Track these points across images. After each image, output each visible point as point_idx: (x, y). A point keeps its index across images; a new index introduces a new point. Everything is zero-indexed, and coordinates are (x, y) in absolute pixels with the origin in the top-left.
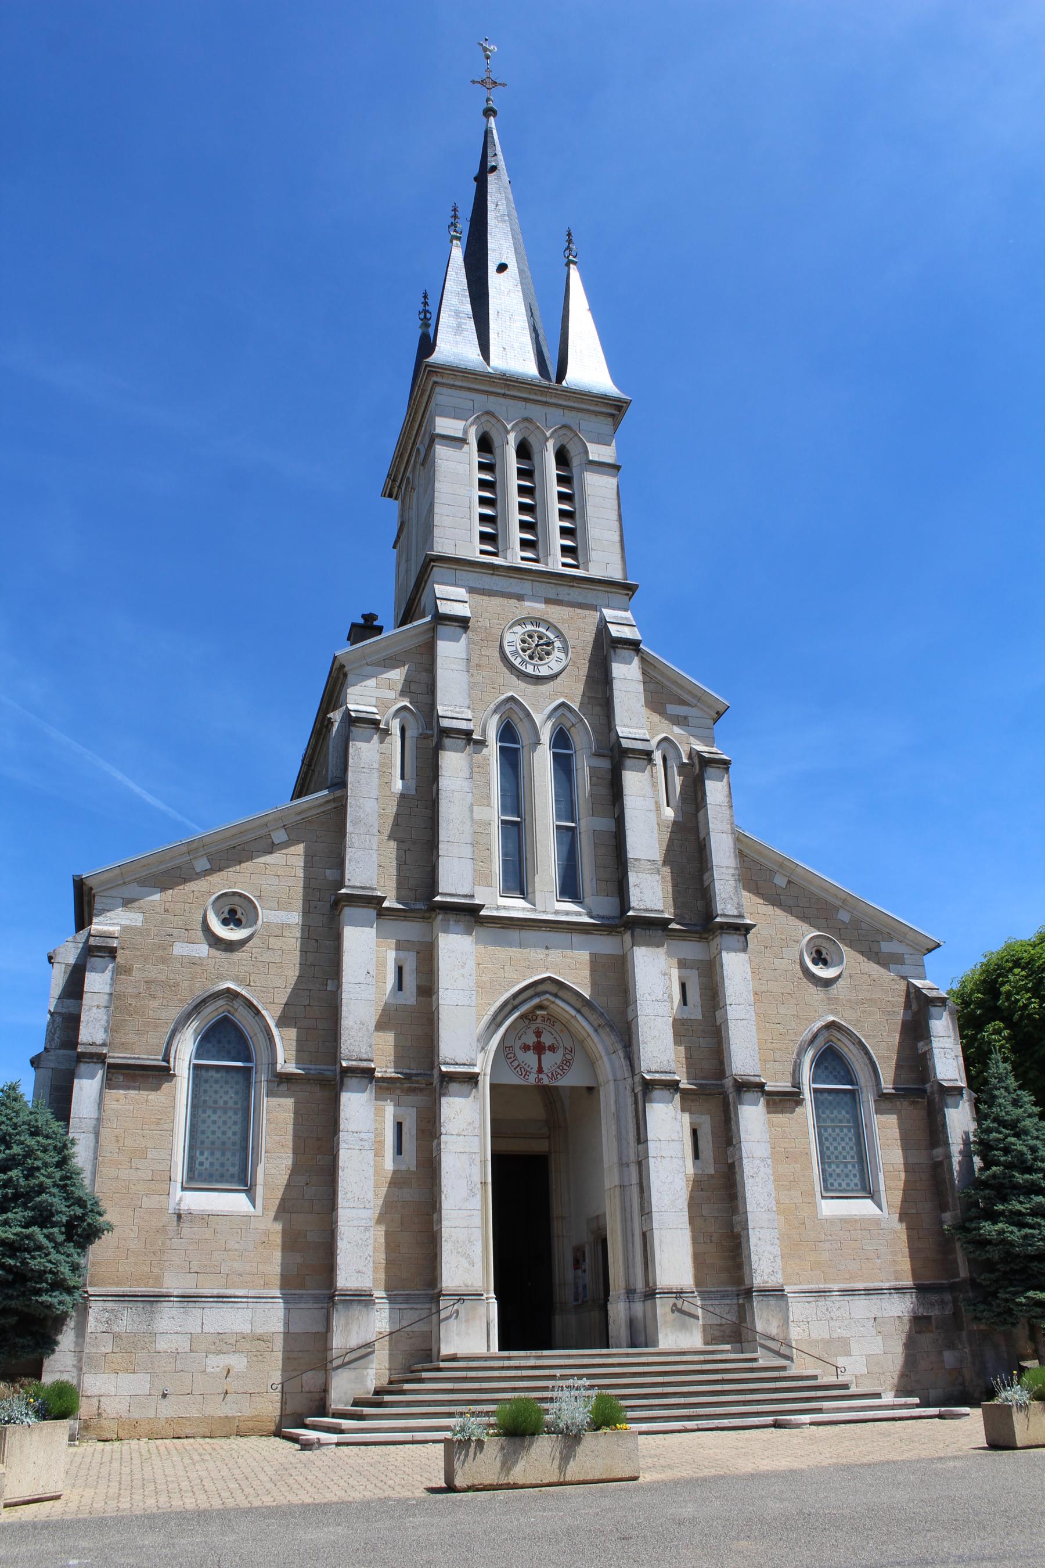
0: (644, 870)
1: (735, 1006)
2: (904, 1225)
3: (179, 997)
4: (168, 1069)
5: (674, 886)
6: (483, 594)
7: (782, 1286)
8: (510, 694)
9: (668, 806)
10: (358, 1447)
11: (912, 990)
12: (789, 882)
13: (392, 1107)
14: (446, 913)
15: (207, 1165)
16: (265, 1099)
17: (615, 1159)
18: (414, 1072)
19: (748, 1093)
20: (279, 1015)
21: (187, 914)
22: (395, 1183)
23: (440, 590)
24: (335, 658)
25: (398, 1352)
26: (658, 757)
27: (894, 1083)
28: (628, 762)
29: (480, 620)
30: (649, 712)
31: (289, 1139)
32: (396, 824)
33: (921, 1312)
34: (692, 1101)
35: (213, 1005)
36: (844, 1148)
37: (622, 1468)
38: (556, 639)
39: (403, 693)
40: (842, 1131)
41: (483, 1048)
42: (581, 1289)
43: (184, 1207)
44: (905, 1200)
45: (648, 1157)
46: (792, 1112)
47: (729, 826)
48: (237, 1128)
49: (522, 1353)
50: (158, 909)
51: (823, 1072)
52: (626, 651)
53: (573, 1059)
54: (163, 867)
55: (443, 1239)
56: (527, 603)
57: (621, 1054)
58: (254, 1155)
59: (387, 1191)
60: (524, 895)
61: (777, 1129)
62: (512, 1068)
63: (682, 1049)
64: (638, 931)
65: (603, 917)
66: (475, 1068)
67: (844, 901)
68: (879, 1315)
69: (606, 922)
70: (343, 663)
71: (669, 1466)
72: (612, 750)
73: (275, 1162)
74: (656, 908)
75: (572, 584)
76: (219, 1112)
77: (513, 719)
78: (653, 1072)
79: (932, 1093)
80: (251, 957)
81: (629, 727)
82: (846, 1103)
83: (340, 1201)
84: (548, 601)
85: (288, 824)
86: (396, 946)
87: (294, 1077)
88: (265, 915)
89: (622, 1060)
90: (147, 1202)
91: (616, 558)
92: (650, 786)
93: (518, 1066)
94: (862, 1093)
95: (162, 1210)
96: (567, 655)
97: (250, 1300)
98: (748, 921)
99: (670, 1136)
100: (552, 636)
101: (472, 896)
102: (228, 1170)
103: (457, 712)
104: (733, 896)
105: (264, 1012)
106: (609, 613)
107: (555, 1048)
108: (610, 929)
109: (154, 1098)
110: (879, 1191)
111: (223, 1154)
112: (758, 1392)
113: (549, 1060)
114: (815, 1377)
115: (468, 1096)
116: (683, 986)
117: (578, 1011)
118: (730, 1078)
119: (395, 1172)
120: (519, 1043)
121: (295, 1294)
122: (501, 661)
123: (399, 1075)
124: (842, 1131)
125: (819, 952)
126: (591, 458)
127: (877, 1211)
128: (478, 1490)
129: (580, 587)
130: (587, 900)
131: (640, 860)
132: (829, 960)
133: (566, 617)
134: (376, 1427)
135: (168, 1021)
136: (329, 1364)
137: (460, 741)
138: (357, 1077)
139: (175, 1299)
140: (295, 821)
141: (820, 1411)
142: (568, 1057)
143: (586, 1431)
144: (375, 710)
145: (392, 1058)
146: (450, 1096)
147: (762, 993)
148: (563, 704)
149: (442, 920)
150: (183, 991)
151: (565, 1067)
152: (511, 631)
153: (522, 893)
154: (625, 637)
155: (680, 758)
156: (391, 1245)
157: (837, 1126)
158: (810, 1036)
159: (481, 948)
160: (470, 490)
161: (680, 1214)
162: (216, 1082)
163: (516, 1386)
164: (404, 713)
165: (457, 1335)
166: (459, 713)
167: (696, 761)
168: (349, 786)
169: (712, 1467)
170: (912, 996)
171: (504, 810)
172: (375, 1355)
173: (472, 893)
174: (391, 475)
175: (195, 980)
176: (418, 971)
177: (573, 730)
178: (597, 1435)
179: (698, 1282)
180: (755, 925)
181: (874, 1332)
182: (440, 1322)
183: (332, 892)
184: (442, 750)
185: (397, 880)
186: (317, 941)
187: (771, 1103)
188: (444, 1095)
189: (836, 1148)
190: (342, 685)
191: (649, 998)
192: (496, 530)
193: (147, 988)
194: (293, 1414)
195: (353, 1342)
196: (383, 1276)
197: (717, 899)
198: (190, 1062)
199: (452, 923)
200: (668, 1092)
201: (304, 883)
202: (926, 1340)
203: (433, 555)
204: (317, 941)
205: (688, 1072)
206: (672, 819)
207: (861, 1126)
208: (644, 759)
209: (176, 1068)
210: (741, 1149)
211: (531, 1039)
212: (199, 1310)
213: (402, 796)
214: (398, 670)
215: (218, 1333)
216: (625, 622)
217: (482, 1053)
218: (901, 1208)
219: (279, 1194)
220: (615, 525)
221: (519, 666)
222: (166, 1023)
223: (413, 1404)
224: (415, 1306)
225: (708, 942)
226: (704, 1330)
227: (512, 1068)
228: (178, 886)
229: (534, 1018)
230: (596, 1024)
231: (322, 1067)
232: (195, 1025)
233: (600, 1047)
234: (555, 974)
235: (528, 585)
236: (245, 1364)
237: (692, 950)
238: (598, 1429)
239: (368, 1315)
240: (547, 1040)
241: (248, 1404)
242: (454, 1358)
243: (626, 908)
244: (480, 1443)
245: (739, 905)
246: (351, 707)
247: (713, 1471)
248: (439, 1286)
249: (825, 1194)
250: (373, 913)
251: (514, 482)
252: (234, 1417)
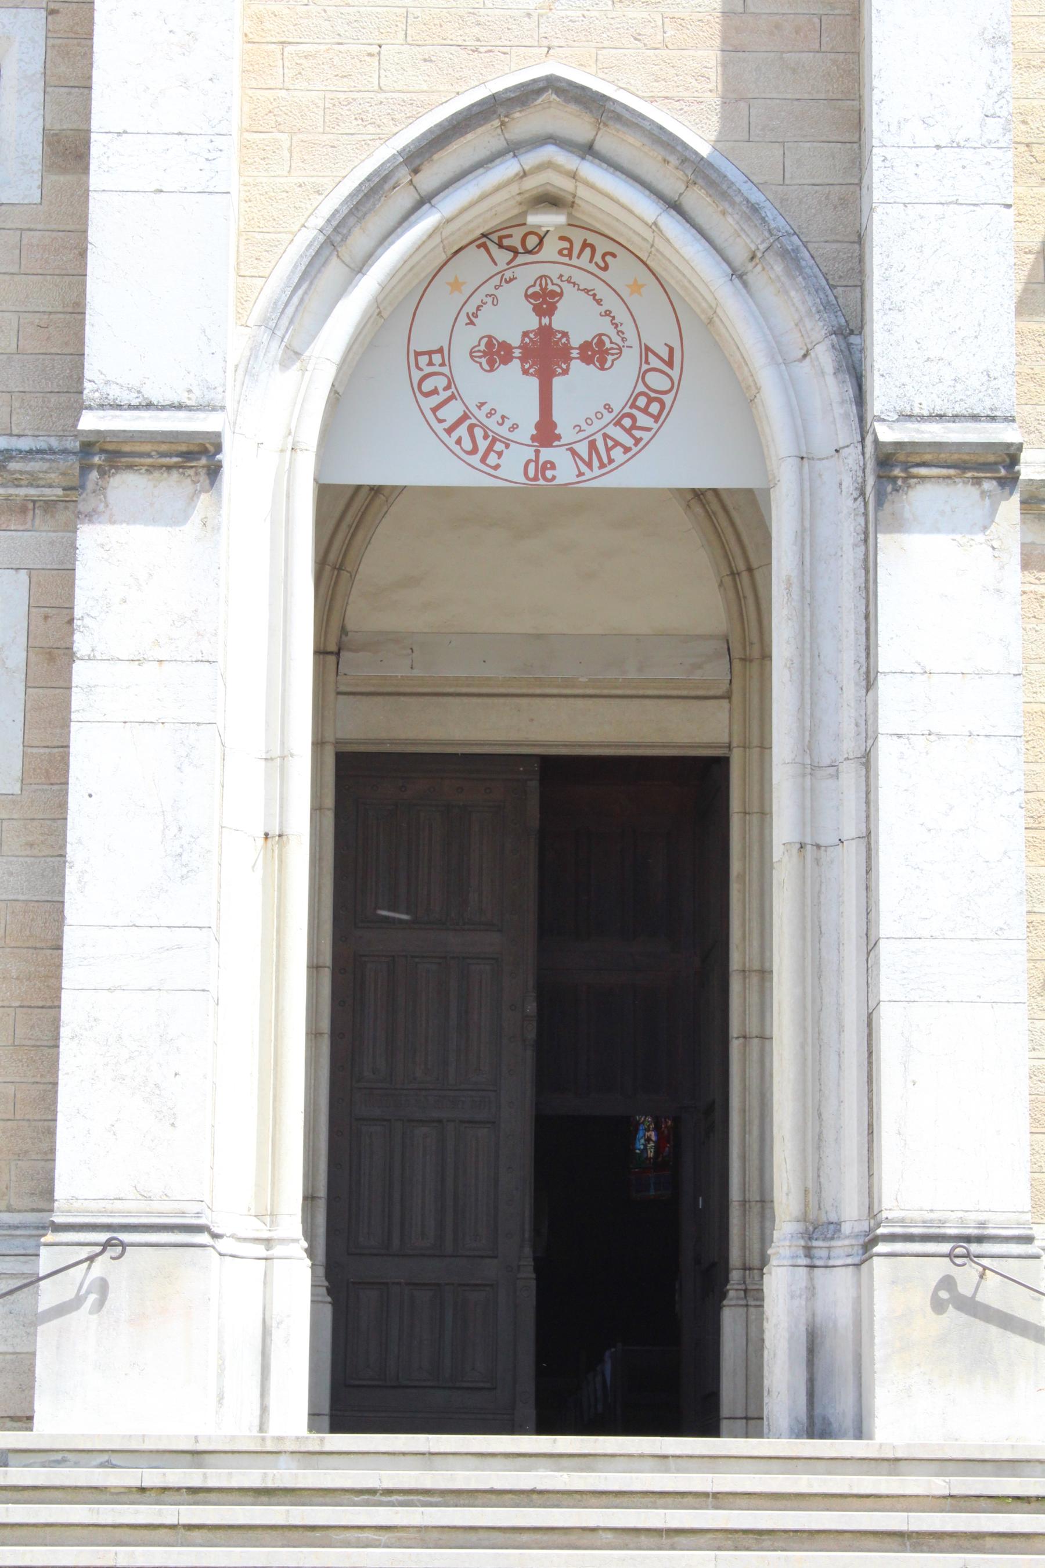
18: (24, 444)
53: (674, 387)
55: (64, 1032)
57: (825, 356)
62: (439, 428)
78: (922, 418)
89: (831, 381)
93: (465, 417)
107: (607, 352)
115: (179, 519)
117: (675, 206)
120: (468, 338)
146: (112, 522)
151: (643, 420)
182: (33, 1321)
188: (90, 517)
200: (973, 491)
229: (532, 242)
230: (739, 253)
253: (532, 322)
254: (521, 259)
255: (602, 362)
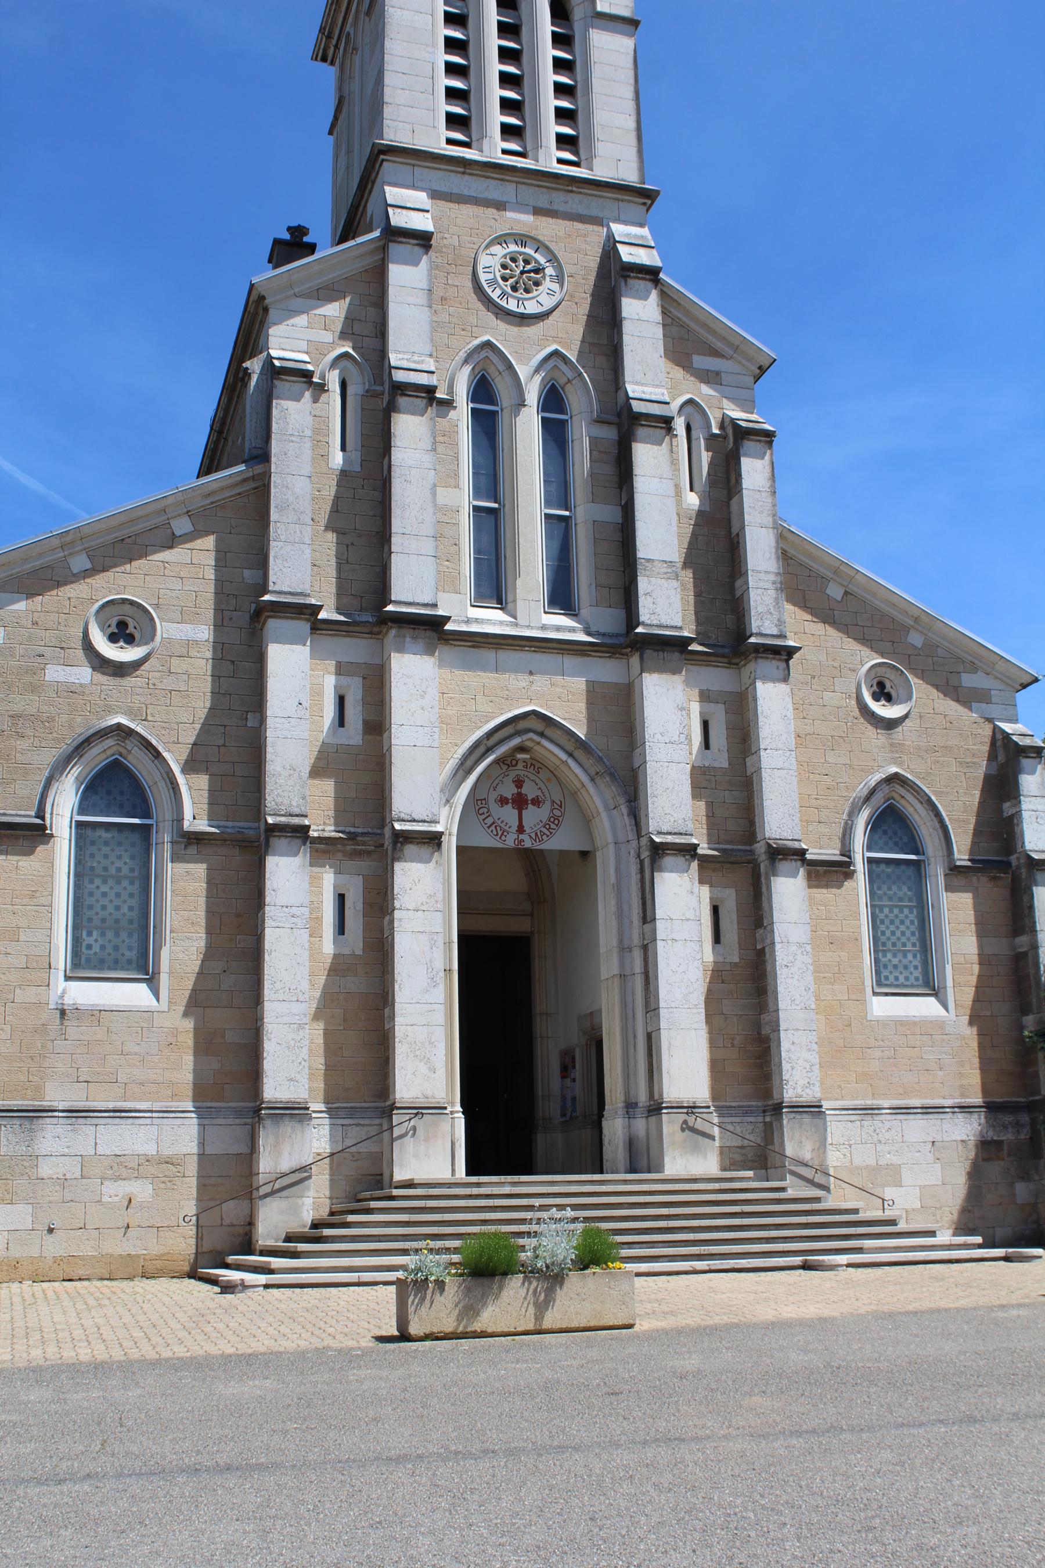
0: (658, 573)
1: (771, 751)
2: (975, 1030)
3: (55, 735)
4: (43, 828)
5: (697, 595)
6: (451, 201)
7: (820, 1101)
8: (485, 338)
9: (691, 490)
10: (292, 1289)
11: (999, 736)
12: (846, 593)
13: (332, 876)
14: (400, 627)
15: (96, 948)
16: (170, 864)
17: (614, 942)
18: (360, 830)
19: (784, 862)
20: (185, 758)
21: (62, 628)
22: (335, 970)
23: (393, 194)
24: (252, 286)
25: (341, 1177)
26: (679, 425)
27: (971, 854)
28: (641, 432)
29: (446, 235)
30: (670, 365)
31: (200, 915)
32: (335, 510)
33: (991, 1135)
34: (714, 870)
35: (100, 746)
36: (903, 933)
37: (614, 1313)
38: (547, 264)
39: (344, 335)
40: (901, 911)
41: (448, 801)
42: (569, 1103)
43: (68, 1001)
44: (977, 1000)
45: (655, 940)
46: (840, 887)
47: (770, 519)
48: (134, 902)
49: (495, 1179)
50: (24, 622)
51: (881, 838)
52: (641, 282)
54: (29, 566)
55: (397, 1040)
56: (509, 214)
58: (157, 935)
59: (326, 980)
60: (502, 604)
61: (819, 908)
62: (485, 826)
63: (702, 804)
64: (648, 653)
65: (604, 635)
66: (438, 825)
67: (917, 619)
68: (939, 1138)
69: (608, 641)
70: (263, 293)
71: (672, 1313)
72: (619, 414)
73: (183, 944)
74: (673, 623)
75: (570, 188)
76: (111, 882)
77: (489, 371)
78: (664, 834)
79: (1018, 867)
80: (148, 684)
81: (642, 385)
82: (909, 878)
83: (266, 992)
84: (537, 211)
85: (193, 510)
86: (336, 669)
87: (206, 837)
88: (164, 629)
89: (626, 817)
90: (20, 996)
91: (631, 153)
92: (669, 463)
93: (494, 823)
94: (929, 865)
95: (41, 1005)
96: (562, 286)
97: (154, 1115)
98: (791, 643)
99: (683, 915)
100: (542, 260)
101: (435, 606)
102: (123, 955)
103: (414, 362)
104: (772, 610)
105: (165, 754)
106: (619, 230)
107: (540, 802)
108: (612, 650)
109: (27, 865)
110: (945, 988)
111: (117, 935)
112: (785, 1227)
113: (533, 816)
114: (856, 1211)
115: (428, 861)
116: (705, 725)
118: (762, 843)
119: (336, 956)
120: (494, 795)
121: (211, 1108)
122: (475, 293)
123: (341, 835)
124: (901, 911)
125: (881, 685)
126: (599, 9)
127: (942, 1011)
128: (437, 1339)
129: (581, 193)
130: (585, 612)
131: (653, 561)
132: (894, 694)
133: (561, 234)
134: (314, 1266)
135: (41, 766)
136: (255, 1192)
137: (419, 400)
138: (286, 837)
139: (61, 1114)
140: (203, 506)
141: (859, 1250)
142: (557, 813)
143: (570, 1270)
144: (306, 358)
145: (332, 813)
147: (806, 735)
148: (556, 353)
149: (395, 636)
150: (60, 727)
151: (553, 826)
152: (488, 252)
153: (500, 602)
154: (640, 262)
155: (709, 427)
156: (332, 1048)
157: (896, 906)
158: (865, 792)
159: (446, 672)
160: (433, 53)
161: (694, 1011)
162: (106, 843)
163: (487, 1218)
164: (345, 363)
165: (414, 1156)
166: (418, 363)
167: (730, 431)
168: (273, 459)
169: (724, 1314)
170: (999, 743)
171: (477, 493)
172: (311, 1181)
173: (434, 602)
174: (325, 29)
175: (74, 713)
176: (365, 702)
177: (568, 388)
178: (585, 1277)
179: (715, 1095)
180: (800, 648)
181: (931, 1158)
183: (252, 599)
184: (395, 411)
185: (337, 583)
186: (233, 662)
187: (813, 875)
188: (398, 859)
189: (893, 933)
190: (262, 323)
191: (661, 739)
192: (469, 110)
193: (13, 724)
194: (211, 1251)
195: (285, 1165)
196: (322, 1085)
197: (753, 614)
198: (71, 818)
199: (408, 640)
200: (683, 859)
201: (216, 588)
202: (995, 1169)
203: (383, 144)
204: (233, 662)
205: (709, 835)
206: (696, 508)
207: (926, 907)
208: (661, 428)
209: (54, 826)
210: (773, 931)
211: (509, 790)
212: (91, 1127)
213: (344, 473)
214: (337, 304)
215: (115, 1155)
216: (640, 242)
217: (447, 808)
218: (972, 1009)
219: (190, 984)
220: (631, 106)
221: (498, 300)
222: (39, 769)
223: (359, 1239)
224: (362, 1122)
225: (739, 668)
226: (721, 1153)
227: (485, 826)
228: (49, 591)
229: (514, 762)
230: (592, 772)
231: (242, 824)
232: (76, 771)
233: (598, 801)
234: (542, 706)
235: (511, 188)
236: (151, 1191)
237: (718, 678)
238: (586, 1267)
239: (303, 1132)
240: (530, 791)
241: (155, 1240)
242: (410, 1185)
243: (634, 624)
244: (440, 1285)
245: (781, 622)
246: (274, 353)
247: (725, 1318)
248: (391, 1097)
249: (877, 990)
250: (305, 627)
251: (493, 42)
252: (138, 1256)
253: (515, 791)
254: (510, 768)
255: (539, 805)
